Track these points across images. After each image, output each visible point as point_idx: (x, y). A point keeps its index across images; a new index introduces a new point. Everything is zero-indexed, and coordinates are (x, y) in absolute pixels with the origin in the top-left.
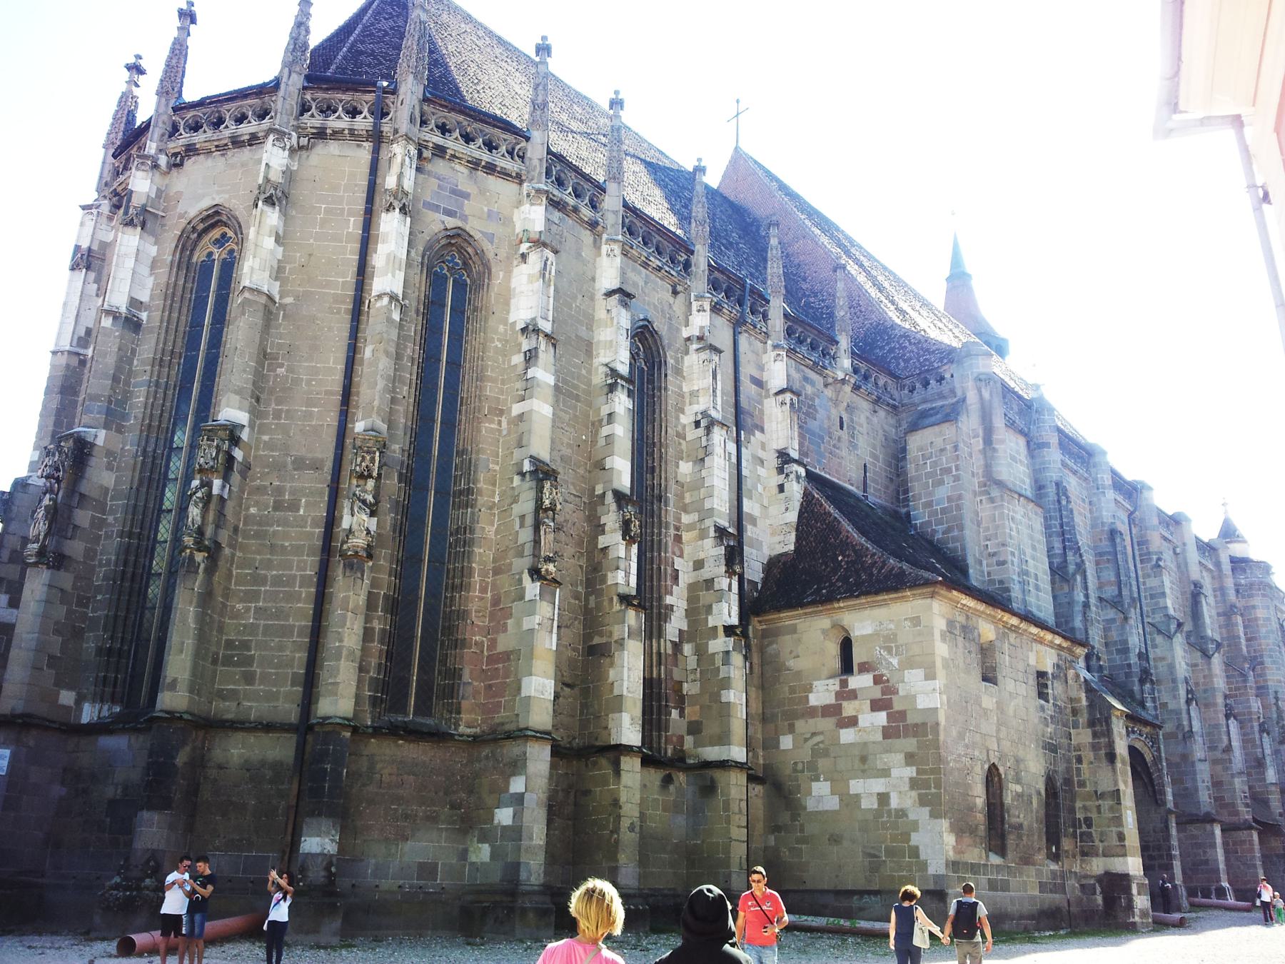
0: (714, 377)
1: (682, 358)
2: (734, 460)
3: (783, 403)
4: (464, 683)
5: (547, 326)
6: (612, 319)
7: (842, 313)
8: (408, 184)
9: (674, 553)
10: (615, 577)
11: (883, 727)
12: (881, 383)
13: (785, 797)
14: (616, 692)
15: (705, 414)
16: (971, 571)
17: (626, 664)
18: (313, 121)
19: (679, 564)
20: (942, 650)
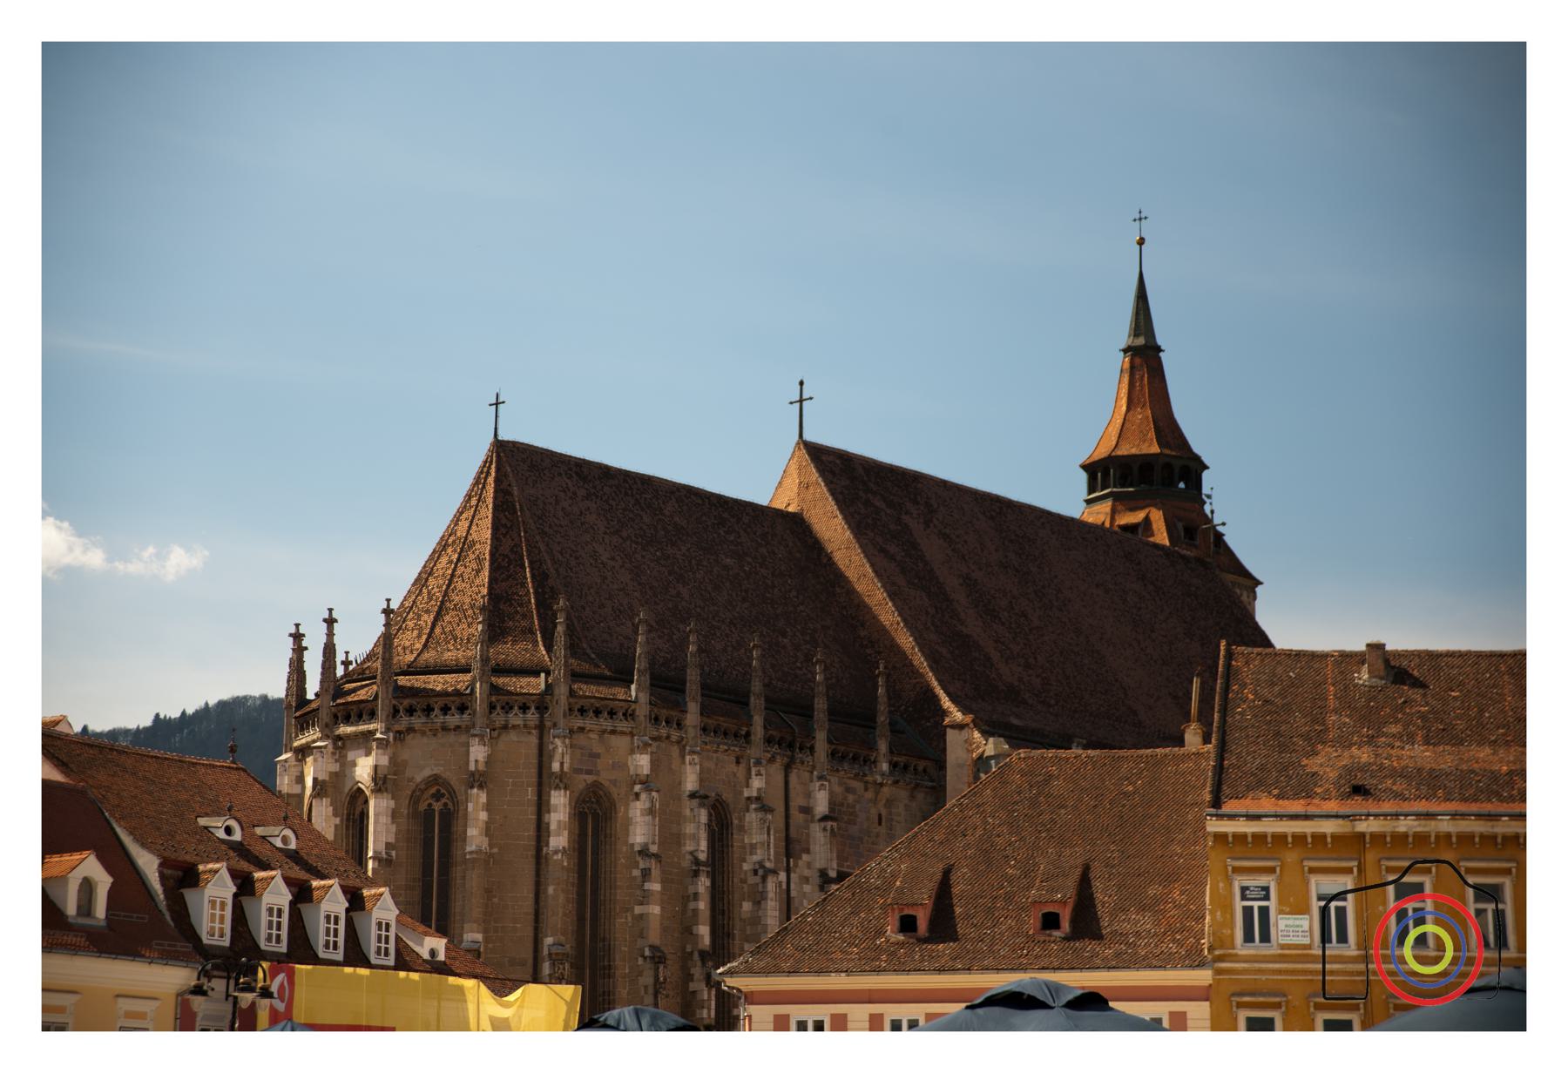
0: (769, 834)
1: (744, 815)
2: (784, 886)
5: (654, 849)
7: (882, 719)
8: (566, 768)
10: (702, 1014)
12: (920, 768)
15: (761, 864)
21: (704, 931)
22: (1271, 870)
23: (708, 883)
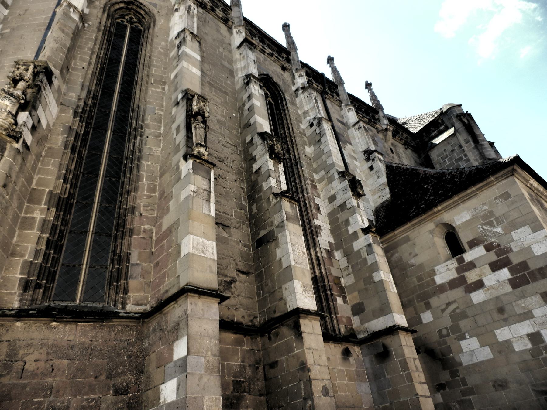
1: (295, 99)
3: (359, 128)
4: (133, 265)
6: (243, 57)
9: (313, 194)
11: (510, 280)
13: (440, 360)
14: (285, 265)
17: (289, 240)
19: (318, 201)
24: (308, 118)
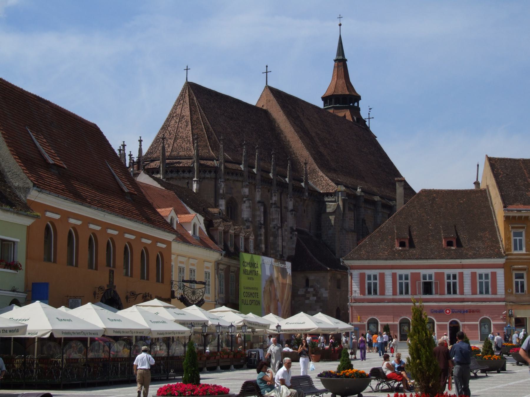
5: (250, 219)
6: (259, 209)
15: (276, 225)
16: (336, 255)
18: (203, 175)
20: (329, 284)
21: (263, 246)
22: (523, 228)
23: (264, 231)
24: (275, 223)
